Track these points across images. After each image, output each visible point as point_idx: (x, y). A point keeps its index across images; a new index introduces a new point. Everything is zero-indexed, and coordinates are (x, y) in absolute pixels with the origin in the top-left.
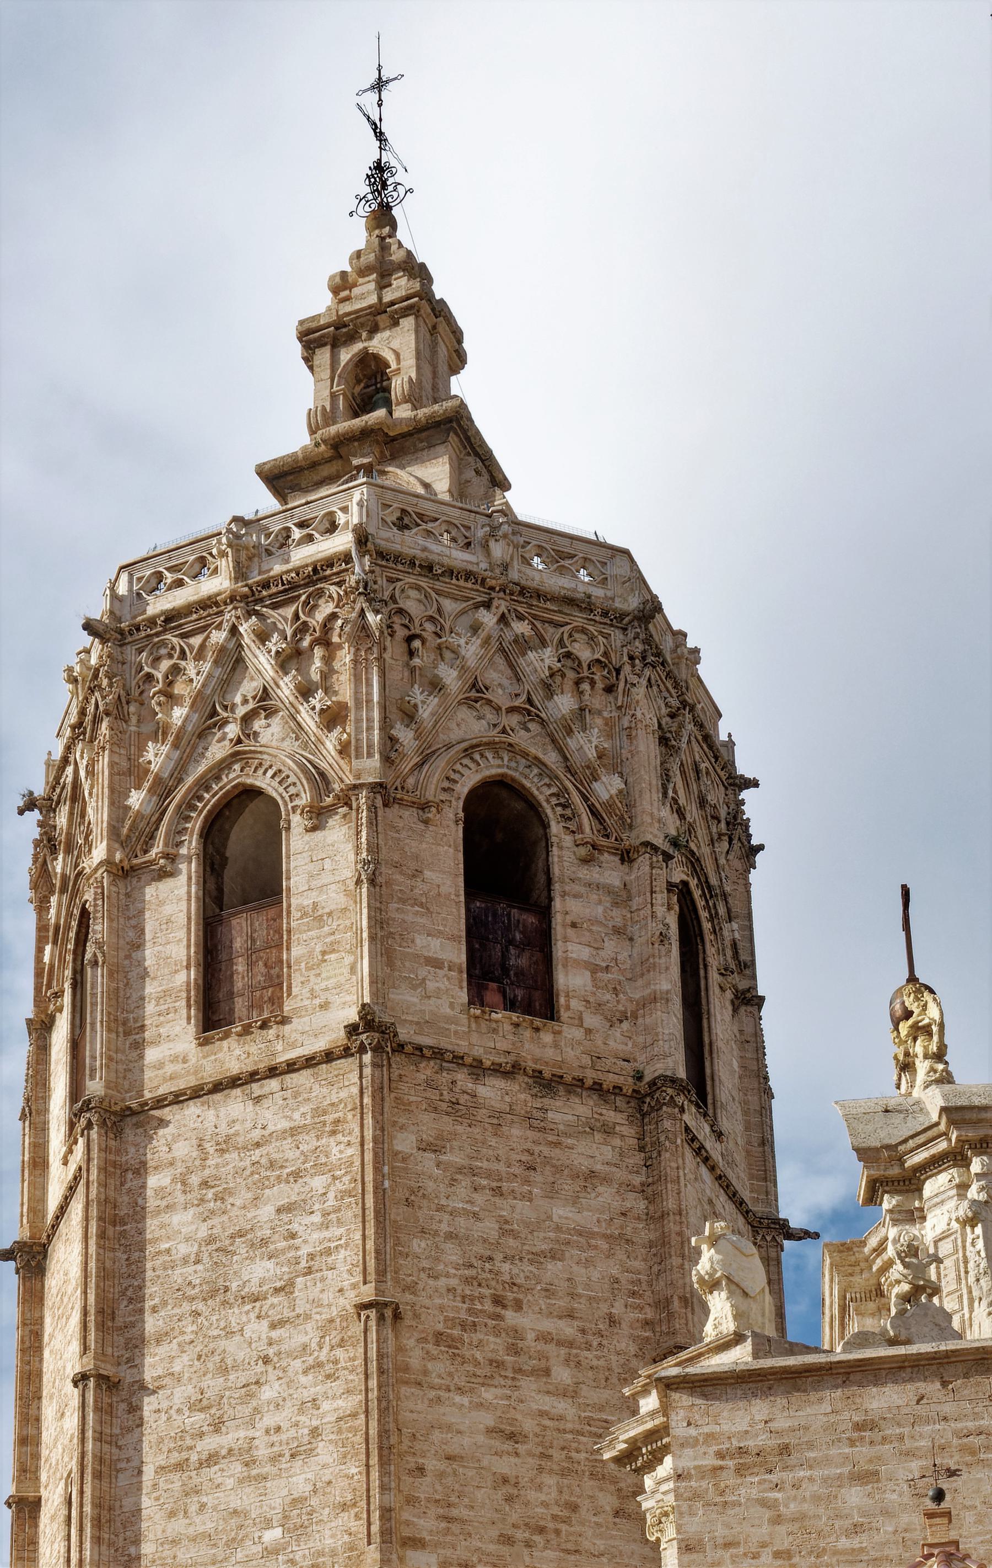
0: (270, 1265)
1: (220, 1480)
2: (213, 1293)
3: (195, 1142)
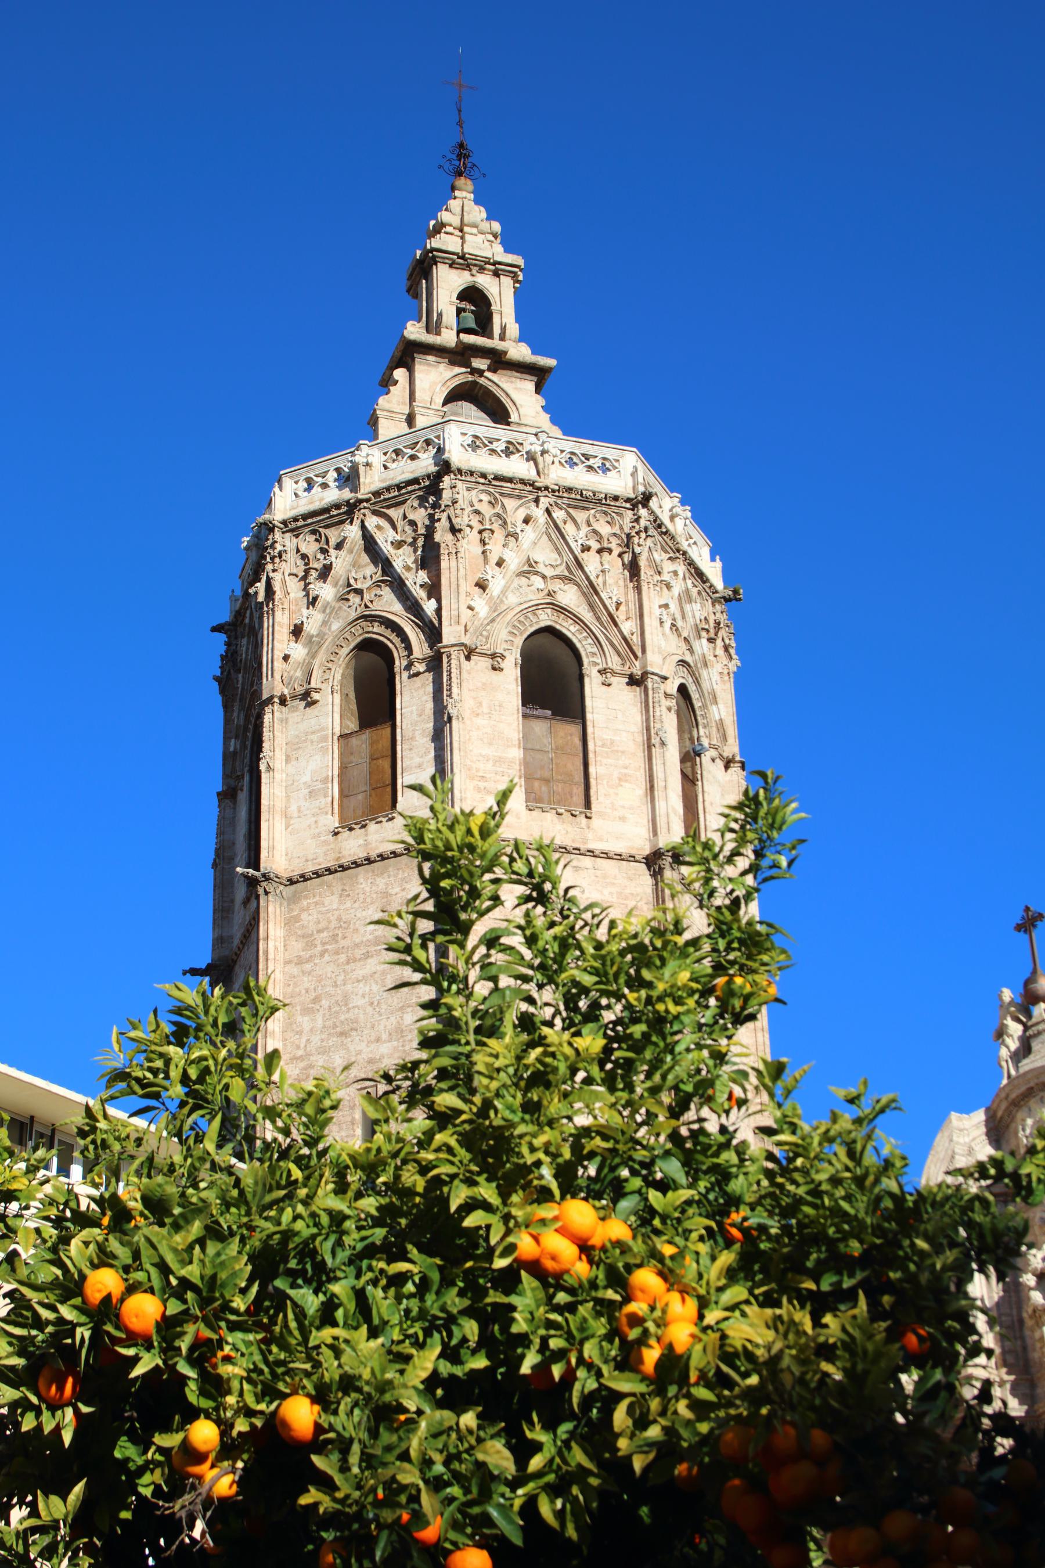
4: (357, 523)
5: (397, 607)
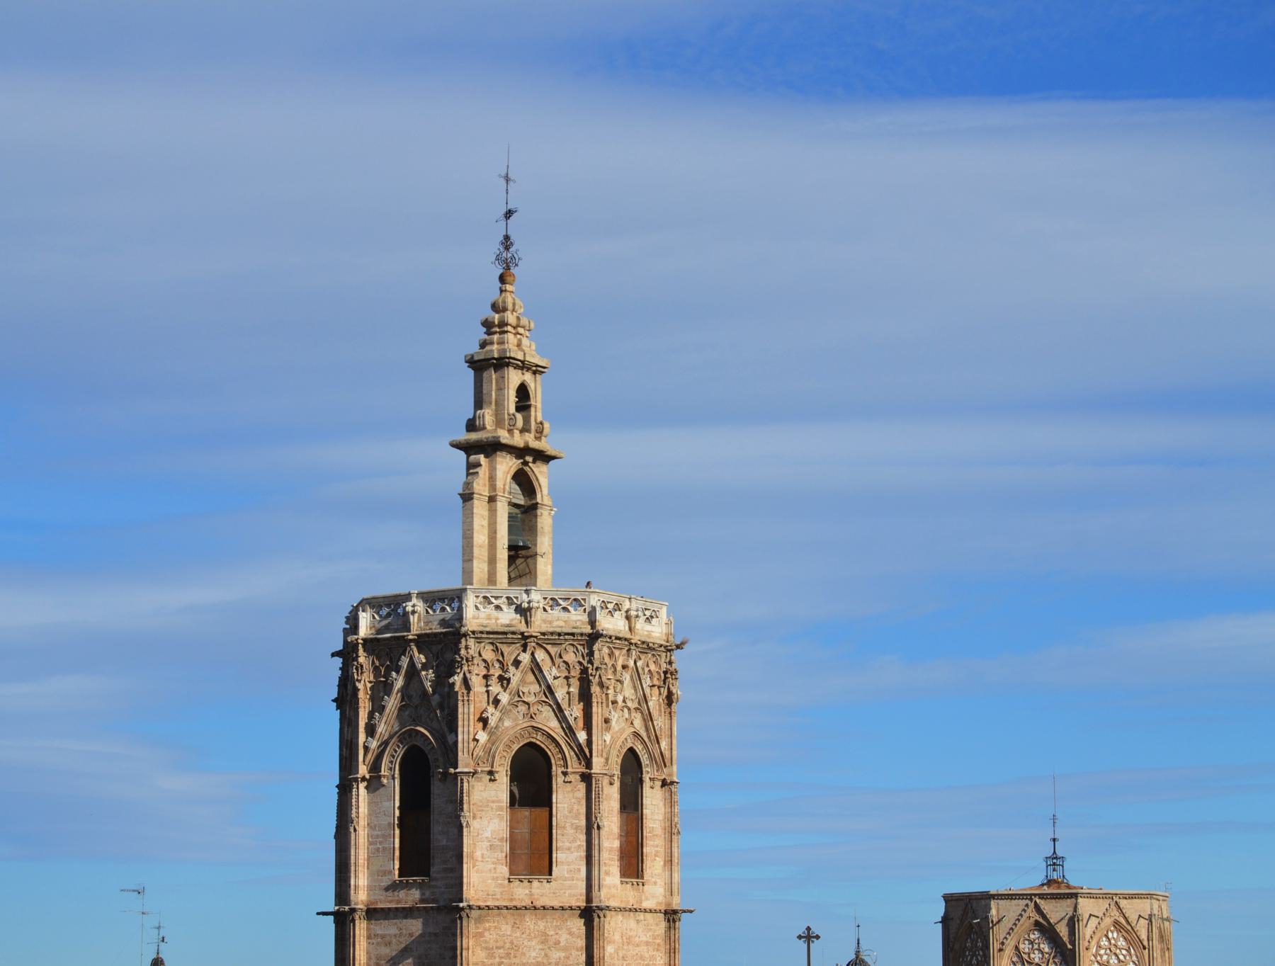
4: (529, 652)
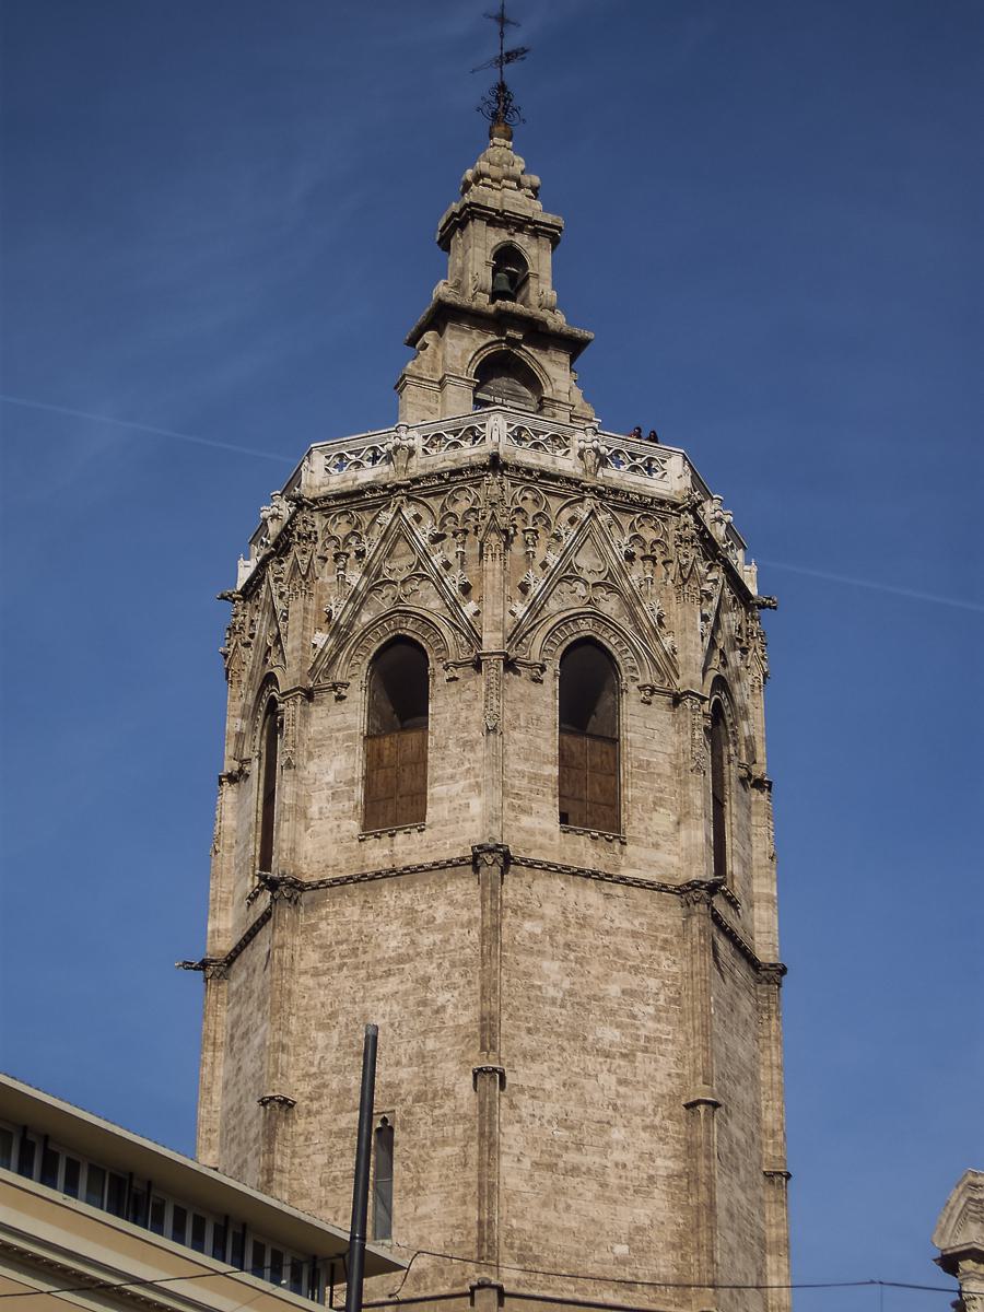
0: (617, 1032)
1: (581, 1191)
2: (574, 1037)
3: (560, 909)
5: (435, 604)
